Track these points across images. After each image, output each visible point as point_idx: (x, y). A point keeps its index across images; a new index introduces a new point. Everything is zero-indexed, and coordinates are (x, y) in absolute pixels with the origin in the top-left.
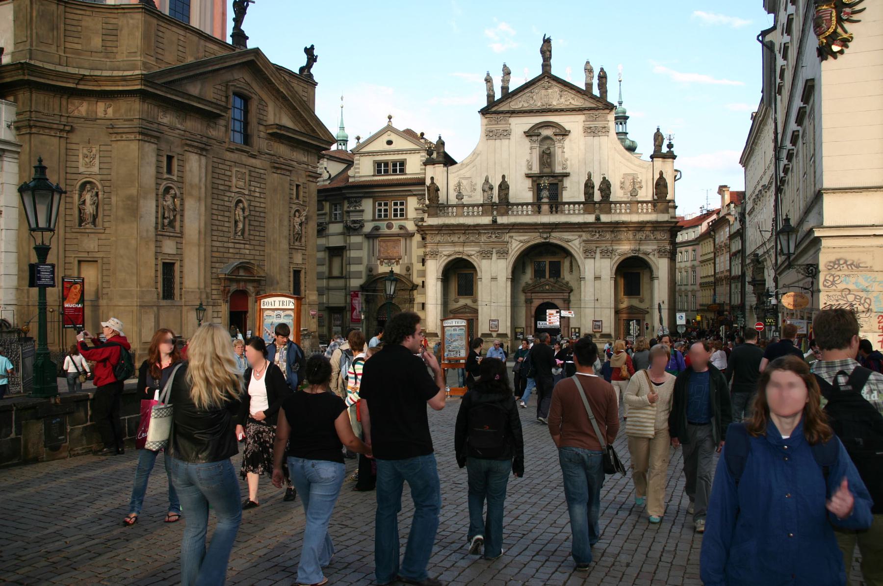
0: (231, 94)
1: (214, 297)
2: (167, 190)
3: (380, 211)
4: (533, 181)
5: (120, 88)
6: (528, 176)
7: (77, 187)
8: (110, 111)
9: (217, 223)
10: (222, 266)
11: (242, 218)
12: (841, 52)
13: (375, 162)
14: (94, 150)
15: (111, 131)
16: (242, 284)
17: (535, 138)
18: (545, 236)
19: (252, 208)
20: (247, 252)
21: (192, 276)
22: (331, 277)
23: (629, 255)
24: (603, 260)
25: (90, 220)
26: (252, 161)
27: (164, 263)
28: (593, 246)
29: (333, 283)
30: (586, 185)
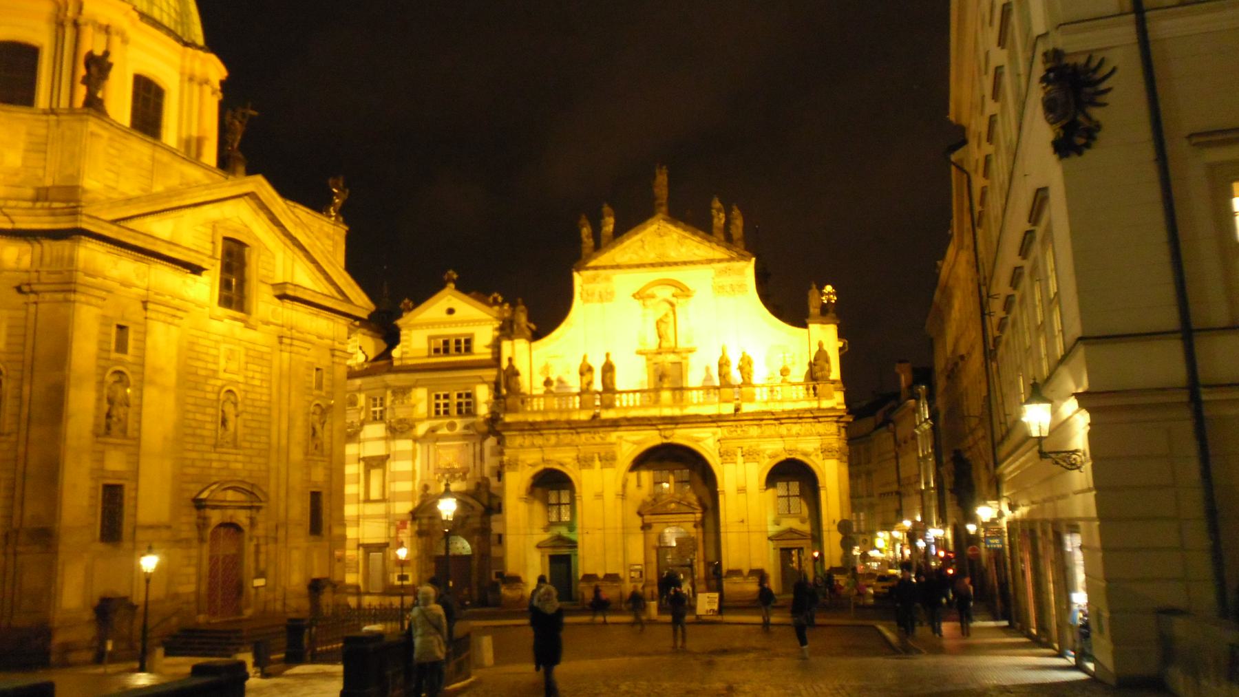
3: (437, 405)
4: (648, 360)
6: (641, 353)
9: (194, 424)
12: (1087, 146)
13: (430, 338)
16: (230, 512)
17: (649, 302)
18: (667, 433)
19: (248, 402)
20: (239, 466)
22: (367, 500)
23: (783, 457)
24: (748, 465)
26: (250, 334)
28: (732, 445)
29: (370, 509)
30: (720, 366)
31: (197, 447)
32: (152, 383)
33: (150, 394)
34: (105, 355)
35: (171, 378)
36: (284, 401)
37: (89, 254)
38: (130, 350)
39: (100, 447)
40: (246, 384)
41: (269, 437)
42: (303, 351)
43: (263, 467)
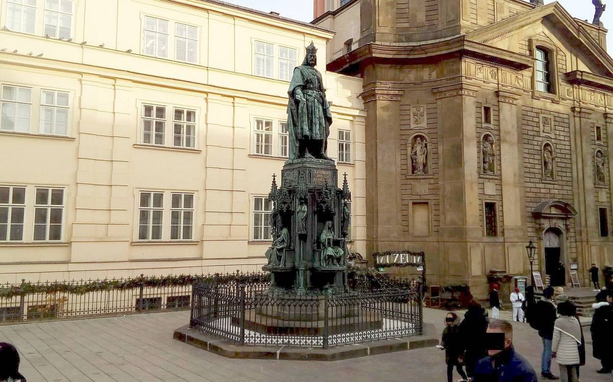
0: (534, 47)
1: (529, 234)
2: (486, 137)
5: (444, 52)
7: (410, 141)
8: (434, 74)
9: (529, 165)
10: (535, 205)
11: (550, 160)
14: (422, 109)
15: (435, 91)
16: (554, 221)
19: (558, 151)
20: (556, 192)
21: (512, 215)
25: (421, 168)
26: (555, 107)
27: (486, 203)
31: (532, 180)
32: (505, 141)
33: (505, 148)
34: (479, 125)
35: (515, 138)
36: (579, 150)
37: (468, 66)
38: (492, 122)
39: (481, 181)
40: (556, 139)
41: (571, 172)
42: (587, 116)
43: (570, 193)
